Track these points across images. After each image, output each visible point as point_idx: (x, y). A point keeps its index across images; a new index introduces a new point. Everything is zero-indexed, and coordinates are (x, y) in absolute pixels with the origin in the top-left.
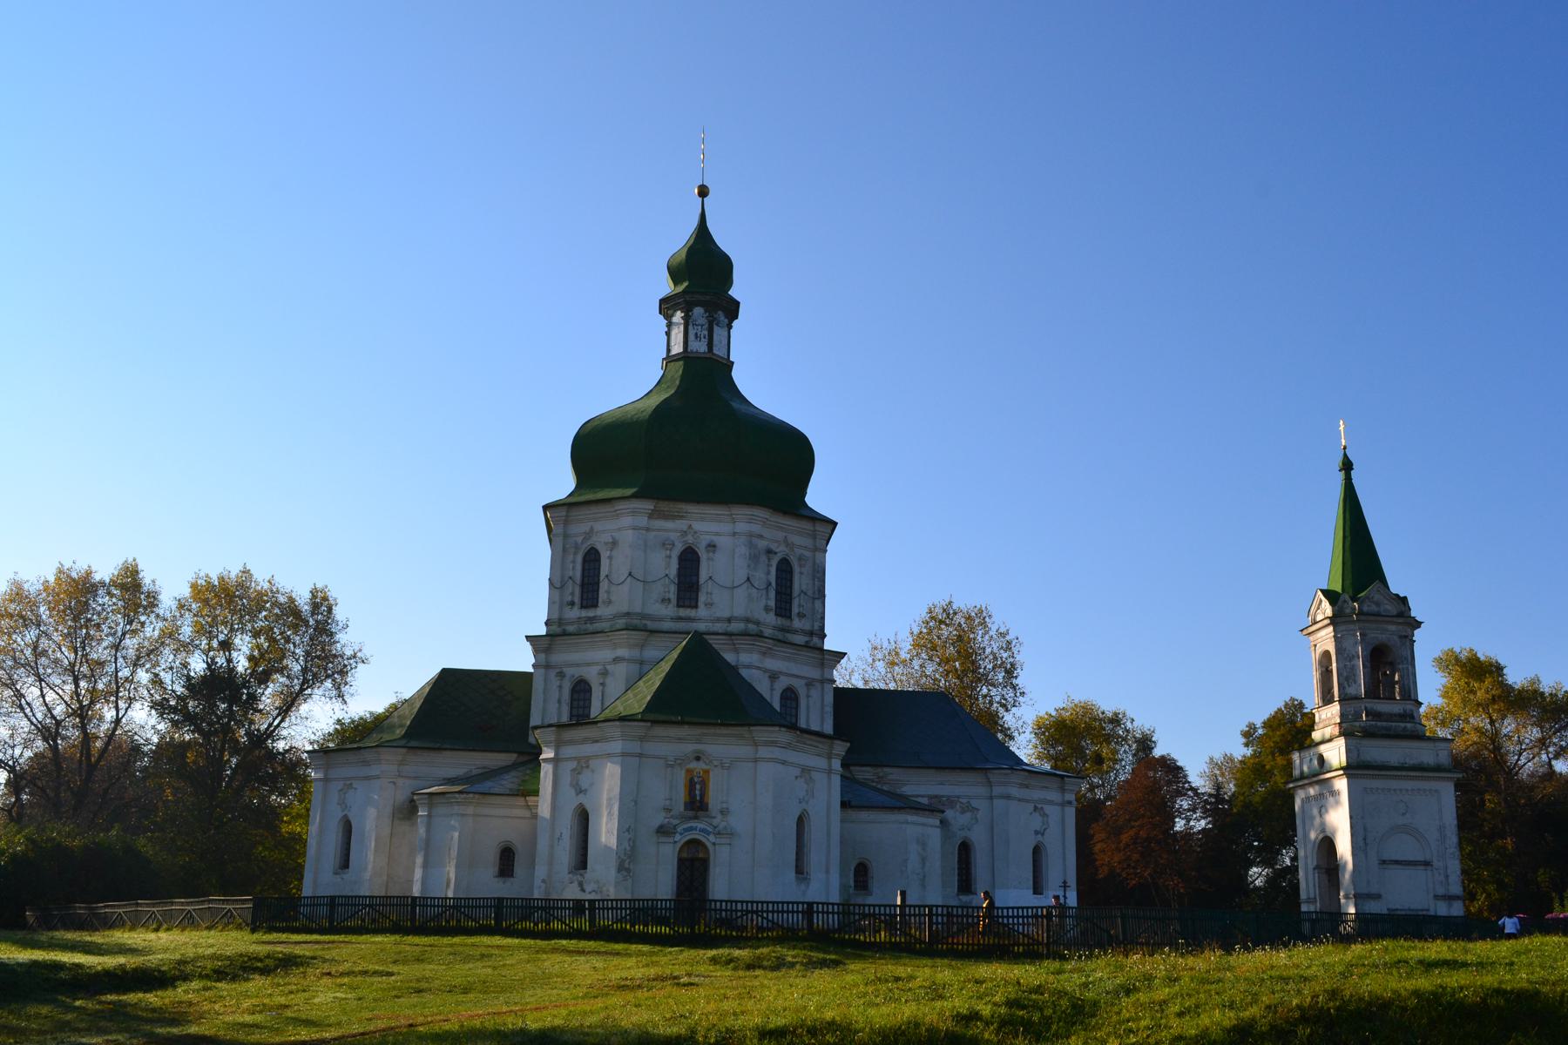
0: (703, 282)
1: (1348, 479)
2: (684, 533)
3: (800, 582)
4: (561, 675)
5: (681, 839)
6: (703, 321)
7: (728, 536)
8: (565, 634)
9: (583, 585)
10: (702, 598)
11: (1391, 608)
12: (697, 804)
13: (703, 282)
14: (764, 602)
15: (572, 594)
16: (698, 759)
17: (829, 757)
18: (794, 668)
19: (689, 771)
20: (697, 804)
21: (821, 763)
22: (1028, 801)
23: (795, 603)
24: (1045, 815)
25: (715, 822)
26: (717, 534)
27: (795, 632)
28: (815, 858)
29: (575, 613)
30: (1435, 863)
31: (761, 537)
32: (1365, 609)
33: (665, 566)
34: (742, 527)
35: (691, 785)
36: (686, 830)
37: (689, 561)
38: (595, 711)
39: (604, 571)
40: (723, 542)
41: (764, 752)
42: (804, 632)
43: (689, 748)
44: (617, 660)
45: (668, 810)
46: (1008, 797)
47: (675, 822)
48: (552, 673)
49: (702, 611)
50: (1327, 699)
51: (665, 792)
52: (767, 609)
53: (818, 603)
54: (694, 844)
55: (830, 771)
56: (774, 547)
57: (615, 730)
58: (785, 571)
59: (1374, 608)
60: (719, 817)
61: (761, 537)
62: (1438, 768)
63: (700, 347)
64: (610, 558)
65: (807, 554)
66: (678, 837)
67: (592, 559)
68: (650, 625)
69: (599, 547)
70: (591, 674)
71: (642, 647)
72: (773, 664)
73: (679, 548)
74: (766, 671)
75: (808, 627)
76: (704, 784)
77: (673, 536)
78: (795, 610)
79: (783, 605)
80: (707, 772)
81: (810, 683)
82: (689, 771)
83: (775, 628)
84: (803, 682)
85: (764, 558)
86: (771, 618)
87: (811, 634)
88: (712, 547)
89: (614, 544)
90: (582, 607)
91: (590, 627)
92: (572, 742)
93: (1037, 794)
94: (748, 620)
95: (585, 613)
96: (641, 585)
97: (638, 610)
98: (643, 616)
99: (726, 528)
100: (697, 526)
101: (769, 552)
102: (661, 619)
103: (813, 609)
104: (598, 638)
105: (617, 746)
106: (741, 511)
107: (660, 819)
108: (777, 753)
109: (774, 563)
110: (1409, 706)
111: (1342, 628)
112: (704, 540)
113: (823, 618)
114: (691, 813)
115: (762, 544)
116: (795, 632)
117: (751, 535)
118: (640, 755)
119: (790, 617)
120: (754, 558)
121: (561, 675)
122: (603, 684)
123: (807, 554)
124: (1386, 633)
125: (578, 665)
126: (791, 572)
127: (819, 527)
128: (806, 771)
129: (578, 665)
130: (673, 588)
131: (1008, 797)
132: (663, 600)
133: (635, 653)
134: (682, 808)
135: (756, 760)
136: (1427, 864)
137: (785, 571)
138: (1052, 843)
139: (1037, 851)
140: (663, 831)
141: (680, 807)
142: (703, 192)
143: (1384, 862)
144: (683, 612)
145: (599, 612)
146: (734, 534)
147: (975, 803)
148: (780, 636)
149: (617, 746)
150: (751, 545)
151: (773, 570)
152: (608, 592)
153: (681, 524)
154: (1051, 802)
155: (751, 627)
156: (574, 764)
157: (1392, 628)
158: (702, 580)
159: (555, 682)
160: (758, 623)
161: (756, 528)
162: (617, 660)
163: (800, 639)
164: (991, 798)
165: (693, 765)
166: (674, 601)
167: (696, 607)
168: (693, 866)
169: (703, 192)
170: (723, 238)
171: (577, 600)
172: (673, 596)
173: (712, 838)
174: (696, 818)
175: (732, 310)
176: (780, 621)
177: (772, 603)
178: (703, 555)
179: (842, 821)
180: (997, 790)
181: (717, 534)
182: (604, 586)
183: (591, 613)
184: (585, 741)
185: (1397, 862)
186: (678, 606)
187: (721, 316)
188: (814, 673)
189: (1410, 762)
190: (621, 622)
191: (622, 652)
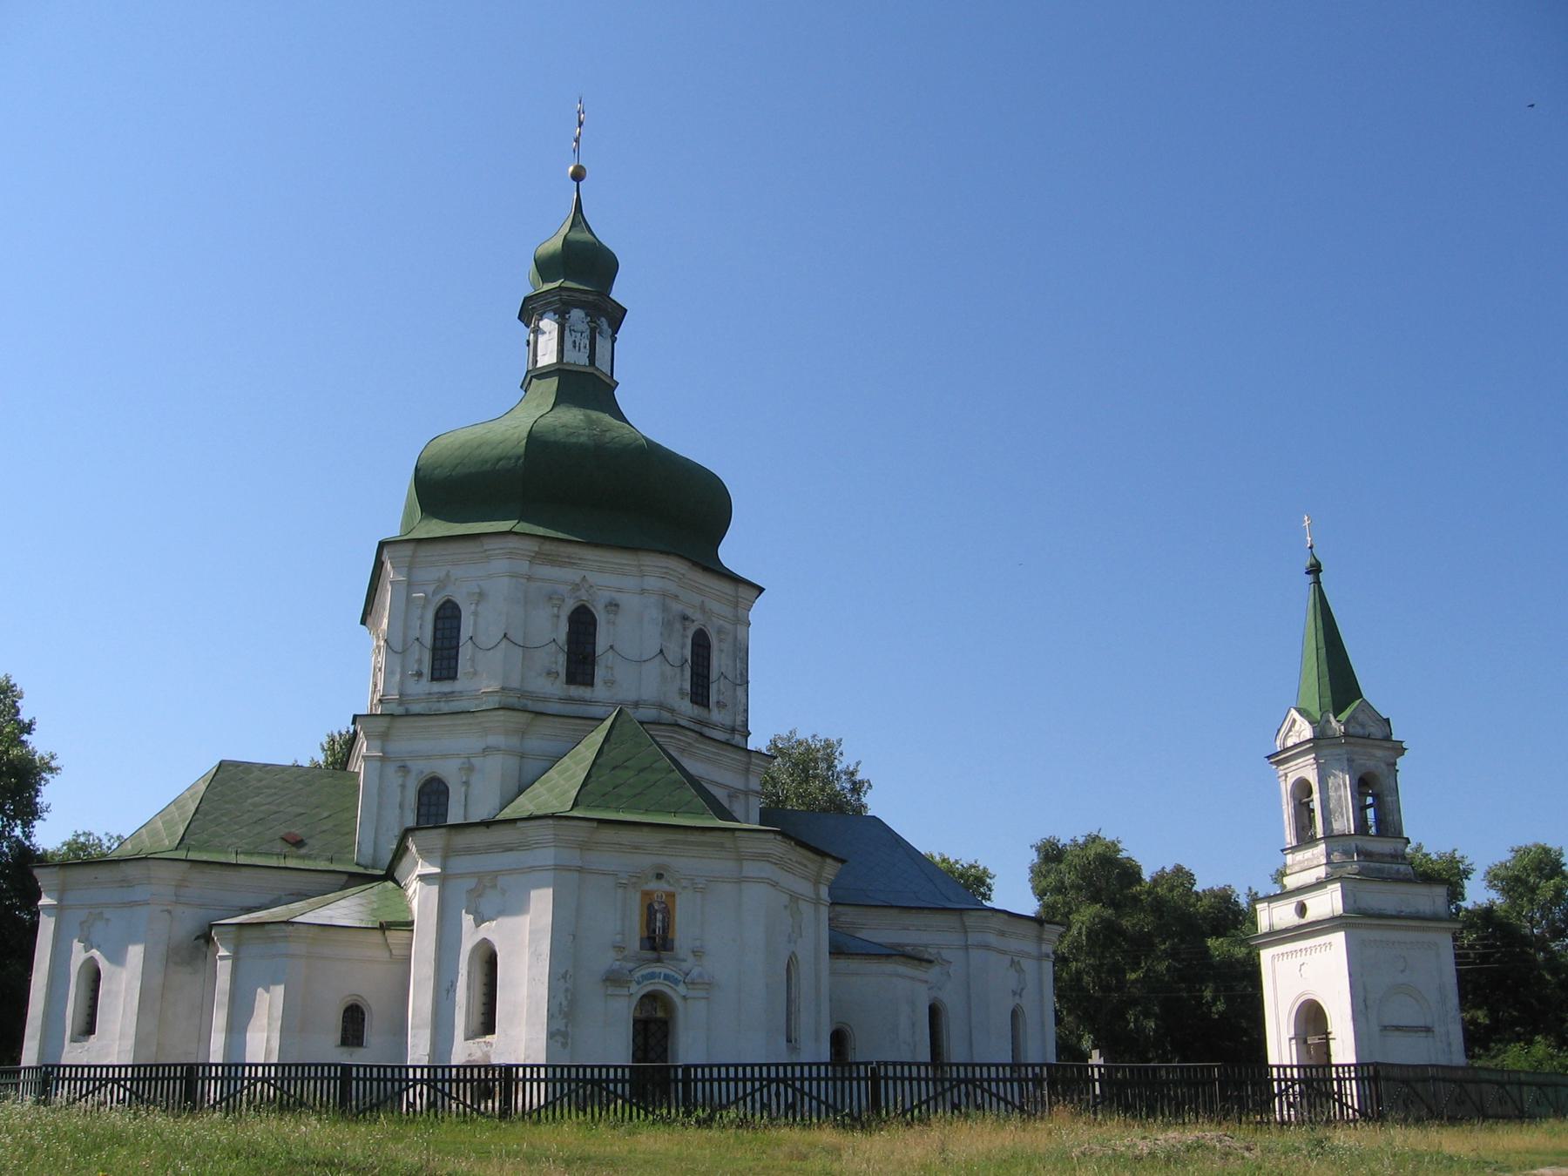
1: (1317, 582)
2: (576, 587)
3: (719, 662)
4: (404, 769)
5: (638, 991)
6: (584, 327)
7: (635, 592)
8: (407, 715)
9: (434, 649)
10: (600, 673)
11: (1376, 731)
12: (657, 941)
15: (420, 661)
16: (659, 876)
17: (817, 883)
19: (647, 894)
20: (657, 941)
21: (805, 888)
22: (1004, 952)
23: (713, 688)
24: (1021, 971)
25: (685, 966)
26: (620, 590)
28: (805, 1020)
29: (425, 686)
30: (1437, 1029)
32: (1351, 730)
33: (552, 629)
34: (652, 583)
35: (650, 912)
36: (645, 977)
37: (582, 625)
38: (452, 819)
39: (466, 630)
40: (630, 602)
41: (751, 869)
42: (724, 728)
43: (646, 861)
44: (487, 751)
45: (619, 948)
46: (987, 947)
47: (631, 965)
48: (391, 769)
49: (599, 691)
50: (1305, 838)
51: (615, 922)
52: (682, 692)
53: (740, 691)
54: (652, 998)
55: (817, 902)
56: (689, 612)
57: (545, 831)
58: (701, 644)
59: (1359, 730)
60: (691, 959)
62: (1435, 918)
63: (578, 358)
64: (475, 614)
65: (728, 626)
66: (634, 988)
67: (448, 617)
68: (530, 705)
69: (458, 599)
70: (449, 771)
71: (523, 734)
73: (570, 605)
75: (728, 721)
76: (668, 913)
78: (713, 698)
80: (672, 895)
82: (647, 894)
83: (691, 719)
85: (678, 626)
86: (686, 707)
87: (733, 730)
88: (613, 606)
89: (481, 596)
90: (433, 679)
91: (445, 707)
92: (470, 851)
93: (1013, 944)
94: (661, 706)
95: (438, 687)
96: (519, 651)
97: (515, 684)
98: (524, 694)
100: (594, 578)
101: (685, 618)
102: (545, 699)
103: (735, 697)
104: (460, 720)
105: (547, 856)
106: (652, 562)
107: (608, 960)
108: (767, 870)
109: (690, 633)
110: (1399, 845)
111: (1326, 752)
114: (650, 954)
115: (676, 607)
116: (714, 726)
117: (664, 595)
118: (580, 870)
120: (667, 624)
121: (404, 769)
122: (467, 783)
123: (728, 626)
124: (1372, 760)
125: (428, 757)
126: (708, 647)
127: (743, 591)
128: (794, 898)
129: (428, 757)
130: (562, 659)
131: (987, 947)
132: (549, 674)
133: (514, 741)
134: (637, 945)
135: (741, 880)
136: (1428, 1030)
137: (701, 644)
138: (1028, 1005)
139: (1015, 1015)
140: (613, 979)
141: (635, 943)
143: (1385, 1028)
144: (575, 691)
145: (457, 686)
146: (643, 591)
147: (946, 954)
148: (697, 727)
149: (547, 856)
150: (665, 609)
151: (689, 642)
152: (472, 659)
154: (1028, 955)
155: (666, 716)
156: (471, 883)
157: (1379, 753)
158: (599, 649)
159: (394, 778)
160: (672, 711)
161: (672, 587)
162: (487, 751)
164: (966, 948)
165: (653, 885)
167: (592, 684)
168: (653, 1027)
170: (607, 233)
171: (426, 670)
173: (682, 989)
174: (659, 960)
175: (616, 315)
176: (696, 711)
177: (687, 686)
178: (601, 617)
179: (833, 973)
180: (973, 938)
181: (620, 590)
182: (465, 652)
183: (446, 687)
184: (489, 849)
185: (1398, 1028)
186: (571, 679)
189: (1407, 910)
190: (493, 702)
191: (492, 740)
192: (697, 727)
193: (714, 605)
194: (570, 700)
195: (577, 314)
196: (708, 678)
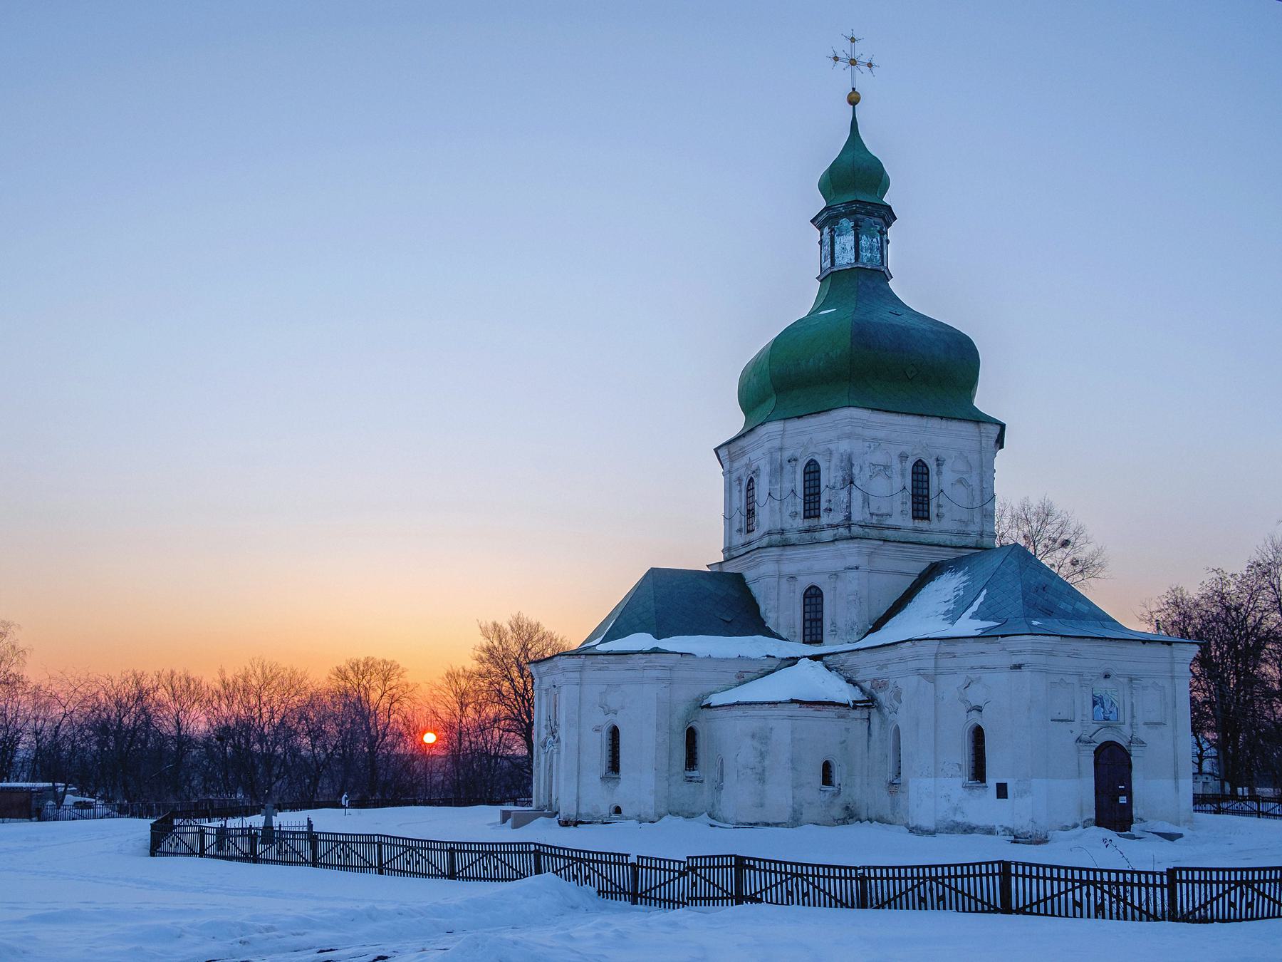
0: (856, 194)
2: (748, 465)
13: (856, 194)
14: (786, 515)
23: (823, 499)
27: (822, 528)
33: (740, 501)
49: (755, 535)
56: (798, 454)
58: (812, 471)
65: (832, 447)
72: (789, 568)
77: (742, 471)
78: (823, 505)
79: (812, 506)
81: (835, 575)
85: (788, 467)
86: (800, 523)
87: (836, 526)
94: (769, 533)
99: (759, 453)
112: (753, 468)
113: (849, 506)
115: (787, 454)
119: (819, 516)
120: (777, 472)
126: (819, 471)
137: (812, 471)
142: (854, 100)
153: (745, 460)
160: (782, 532)
161: (777, 443)
166: (744, 530)
169: (854, 100)
176: (808, 523)
177: (800, 509)
187: (846, 223)
188: (839, 565)
192: (807, 536)
194: (745, 545)
195: (826, 230)
196: (819, 494)
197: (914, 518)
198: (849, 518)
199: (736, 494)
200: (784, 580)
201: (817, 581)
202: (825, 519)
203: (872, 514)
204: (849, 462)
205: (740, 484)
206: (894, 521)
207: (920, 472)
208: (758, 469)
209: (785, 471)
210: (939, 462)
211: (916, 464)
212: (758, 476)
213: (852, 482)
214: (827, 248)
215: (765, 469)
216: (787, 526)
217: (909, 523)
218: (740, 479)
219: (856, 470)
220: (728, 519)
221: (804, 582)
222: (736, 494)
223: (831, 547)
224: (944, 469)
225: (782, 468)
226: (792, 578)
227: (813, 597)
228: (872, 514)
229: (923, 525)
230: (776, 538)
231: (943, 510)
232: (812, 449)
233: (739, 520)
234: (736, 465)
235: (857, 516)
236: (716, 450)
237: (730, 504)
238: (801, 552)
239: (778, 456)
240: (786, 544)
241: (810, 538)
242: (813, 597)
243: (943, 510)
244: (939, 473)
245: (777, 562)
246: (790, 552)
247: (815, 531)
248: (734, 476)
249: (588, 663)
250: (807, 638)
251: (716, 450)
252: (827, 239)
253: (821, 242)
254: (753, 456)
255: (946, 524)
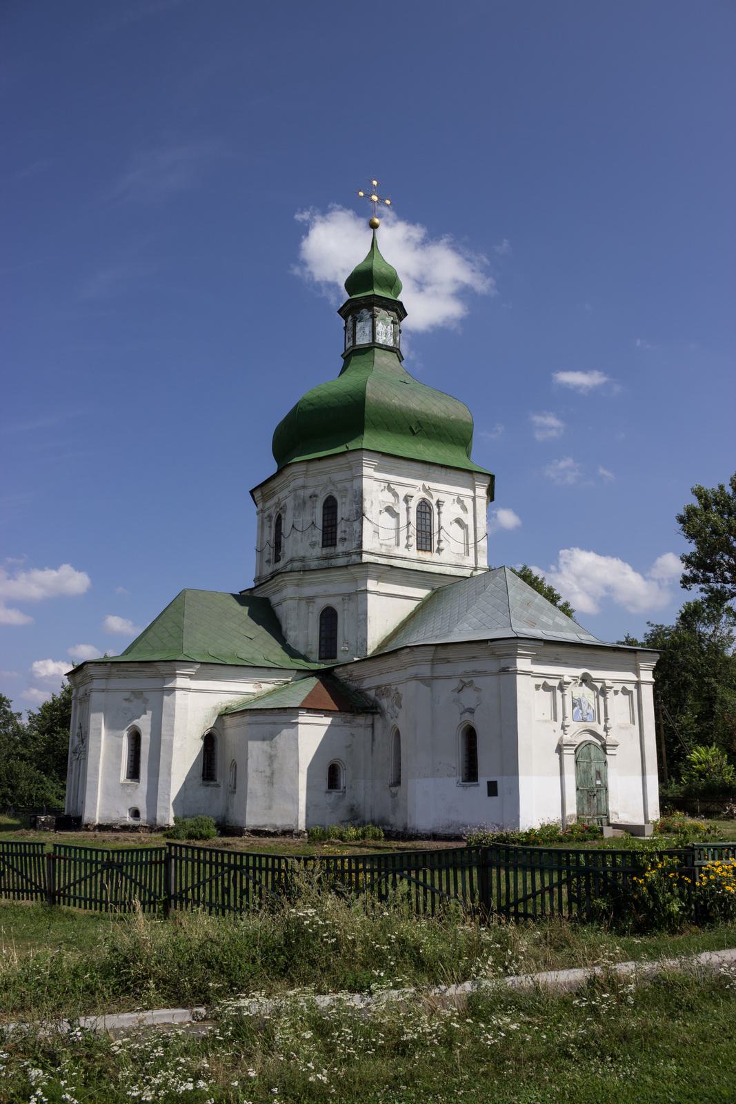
2: (277, 504)
3: (343, 511)
18: (333, 589)
22: (449, 678)
27: (337, 556)
31: (304, 487)
49: (281, 564)
53: (356, 524)
56: (318, 492)
58: (330, 506)
61: (304, 487)
72: (308, 591)
74: (300, 599)
79: (329, 538)
83: (319, 559)
84: (340, 598)
86: (318, 551)
94: (292, 561)
113: (361, 536)
115: (309, 492)
119: (335, 545)
123: (348, 485)
128: (138, 694)
131: (415, 678)
147: (401, 689)
148: (325, 564)
153: (275, 499)
154: (484, 673)
160: (303, 559)
161: (300, 482)
163: (341, 561)
172: (272, 557)
193: (337, 477)
195: (350, 318)
197: (418, 549)
198: (360, 545)
199: (267, 530)
200: (303, 603)
201: (334, 602)
202: (340, 548)
203: (381, 545)
204: (359, 498)
205: (270, 521)
206: (401, 551)
207: (425, 510)
208: (285, 505)
209: (307, 505)
210: (439, 504)
211: (420, 505)
212: (285, 512)
213: (364, 515)
214: (350, 333)
215: (290, 503)
216: (308, 554)
217: (413, 553)
218: (270, 517)
219: (367, 505)
220: (260, 551)
221: (321, 604)
222: (267, 530)
223: (344, 572)
224: (442, 509)
225: (304, 503)
226: (310, 600)
227: (329, 619)
228: (381, 545)
229: (426, 556)
230: (297, 565)
231: (442, 545)
232: (331, 487)
233: (269, 552)
234: (268, 504)
235: (365, 547)
236: (252, 492)
237: (262, 539)
238: (320, 576)
239: (301, 493)
240: (305, 570)
241: (327, 566)
242: (329, 619)
243: (442, 545)
244: (439, 513)
245: (298, 585)
246: (308, 576)
247: (331, 558)
248: (266, 514)
249: (114, 670)
250: (323, 655)
251: (252, 492)
252: (350, 324)
253: (345, 328)
254: (282, 495)
255: (445, 557)
